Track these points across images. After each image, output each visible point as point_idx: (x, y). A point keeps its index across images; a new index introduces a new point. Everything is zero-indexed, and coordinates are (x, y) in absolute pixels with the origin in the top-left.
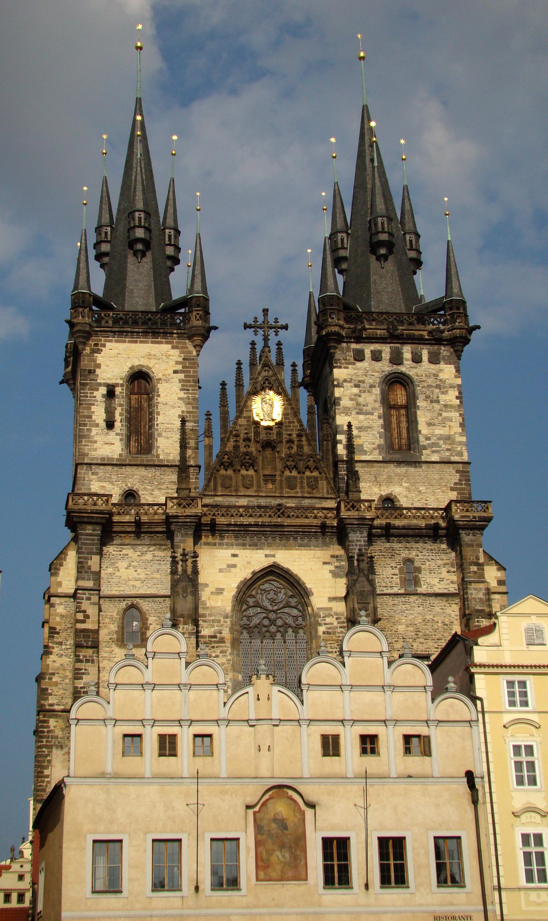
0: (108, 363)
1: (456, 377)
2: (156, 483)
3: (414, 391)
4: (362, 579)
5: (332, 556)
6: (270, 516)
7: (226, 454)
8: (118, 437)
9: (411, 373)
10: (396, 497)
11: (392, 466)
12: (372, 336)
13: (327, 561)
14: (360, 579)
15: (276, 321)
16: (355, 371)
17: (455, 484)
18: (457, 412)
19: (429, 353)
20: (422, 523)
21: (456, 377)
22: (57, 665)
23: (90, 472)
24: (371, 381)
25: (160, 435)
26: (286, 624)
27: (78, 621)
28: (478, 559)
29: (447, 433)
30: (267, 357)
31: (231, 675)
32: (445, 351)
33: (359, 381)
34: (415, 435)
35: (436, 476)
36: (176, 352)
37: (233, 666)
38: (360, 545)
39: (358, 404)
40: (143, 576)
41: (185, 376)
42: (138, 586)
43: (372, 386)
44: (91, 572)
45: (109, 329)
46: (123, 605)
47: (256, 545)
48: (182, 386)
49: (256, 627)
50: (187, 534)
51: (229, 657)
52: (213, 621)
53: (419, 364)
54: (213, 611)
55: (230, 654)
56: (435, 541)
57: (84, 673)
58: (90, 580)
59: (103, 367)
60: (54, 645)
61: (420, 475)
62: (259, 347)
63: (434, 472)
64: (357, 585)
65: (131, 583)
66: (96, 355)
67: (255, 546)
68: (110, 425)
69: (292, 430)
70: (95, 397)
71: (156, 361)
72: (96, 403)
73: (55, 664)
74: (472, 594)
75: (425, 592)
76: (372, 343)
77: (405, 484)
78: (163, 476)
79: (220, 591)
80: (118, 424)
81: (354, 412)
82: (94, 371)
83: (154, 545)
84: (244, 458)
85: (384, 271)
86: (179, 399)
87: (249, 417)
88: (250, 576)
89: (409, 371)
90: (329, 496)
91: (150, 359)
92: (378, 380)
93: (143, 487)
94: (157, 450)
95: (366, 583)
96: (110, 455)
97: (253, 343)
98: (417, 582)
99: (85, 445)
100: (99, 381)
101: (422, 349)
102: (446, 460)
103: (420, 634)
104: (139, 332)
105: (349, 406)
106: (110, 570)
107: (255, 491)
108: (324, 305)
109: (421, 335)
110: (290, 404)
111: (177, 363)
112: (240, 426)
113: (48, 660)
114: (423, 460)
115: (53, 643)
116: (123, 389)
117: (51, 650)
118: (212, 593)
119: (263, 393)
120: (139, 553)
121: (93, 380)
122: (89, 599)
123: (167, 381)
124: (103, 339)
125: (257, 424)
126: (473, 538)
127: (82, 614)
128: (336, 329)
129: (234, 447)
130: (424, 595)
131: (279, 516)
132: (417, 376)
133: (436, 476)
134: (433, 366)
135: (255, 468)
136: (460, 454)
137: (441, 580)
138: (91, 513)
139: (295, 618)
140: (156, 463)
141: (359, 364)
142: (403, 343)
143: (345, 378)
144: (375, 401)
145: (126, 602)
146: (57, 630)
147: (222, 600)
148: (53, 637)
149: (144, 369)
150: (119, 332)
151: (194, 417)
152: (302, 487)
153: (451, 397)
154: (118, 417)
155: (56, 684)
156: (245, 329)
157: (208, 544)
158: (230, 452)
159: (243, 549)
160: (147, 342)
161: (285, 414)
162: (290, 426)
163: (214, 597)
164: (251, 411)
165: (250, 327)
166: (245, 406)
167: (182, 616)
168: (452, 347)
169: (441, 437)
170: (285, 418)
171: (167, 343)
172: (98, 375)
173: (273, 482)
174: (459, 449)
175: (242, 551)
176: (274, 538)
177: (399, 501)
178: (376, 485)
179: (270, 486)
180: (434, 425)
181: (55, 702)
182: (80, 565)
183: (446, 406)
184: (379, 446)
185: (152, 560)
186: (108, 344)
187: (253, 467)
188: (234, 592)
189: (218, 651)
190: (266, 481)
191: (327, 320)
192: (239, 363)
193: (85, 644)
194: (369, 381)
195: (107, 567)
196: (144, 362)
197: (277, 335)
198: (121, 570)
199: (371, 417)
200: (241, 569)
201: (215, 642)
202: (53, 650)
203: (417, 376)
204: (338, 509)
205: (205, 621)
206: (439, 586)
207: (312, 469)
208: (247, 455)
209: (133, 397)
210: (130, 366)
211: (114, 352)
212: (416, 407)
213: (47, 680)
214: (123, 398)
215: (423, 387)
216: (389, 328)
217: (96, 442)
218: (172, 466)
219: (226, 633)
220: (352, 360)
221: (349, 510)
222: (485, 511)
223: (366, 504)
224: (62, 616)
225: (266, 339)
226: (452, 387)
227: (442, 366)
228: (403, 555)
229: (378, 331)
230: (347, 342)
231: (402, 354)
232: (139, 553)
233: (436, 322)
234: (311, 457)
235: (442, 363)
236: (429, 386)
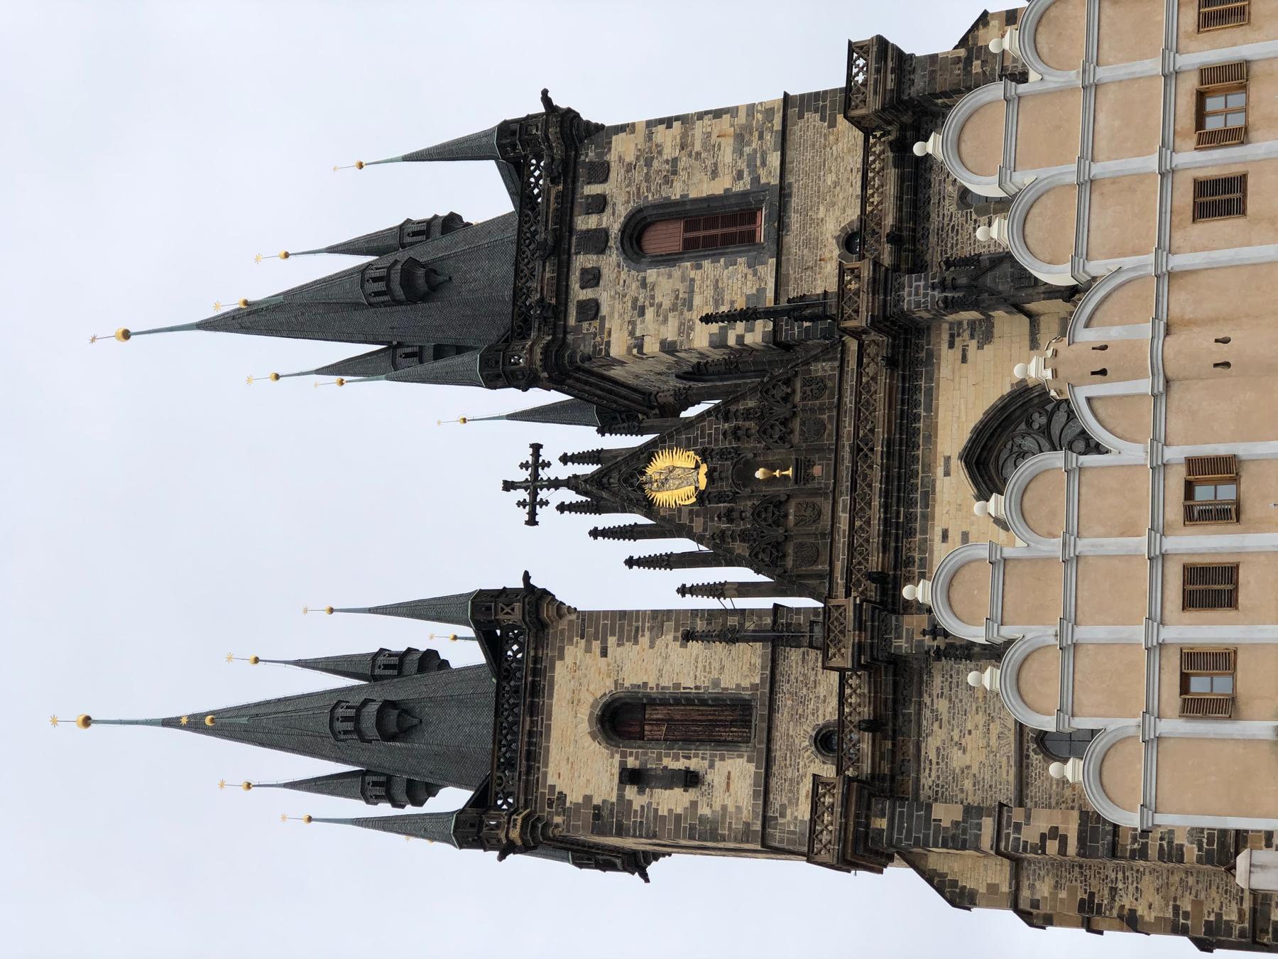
0: (583, 781)
1: (633, 132)
2: (805, 691)
4: (988, 280)
5: (951, 345)
6: (871, 467)
7: (756, 555)
8: (717, 764)
10: (844, 228)
12: (554, 288)
15: (524, 466)
16: (616, 315)
17: (823, 119)
18: (694, 123)
20: (892, 173)
22: (1157, 900)
23: (781, 821)
25: (716, 683)
27: (1063, 850)
29: (731, 141)
30: (586, 481)
32: (590, 155)
33: (634, 308)
34: (733, 201)
36: (570, 651)
38: (926, 288)
39: (674, 308)
40: (981, 719)
41: (613, 634)
42: (999, 729)
43: (644, 284)
44: (964, 821)
45: (524, 777)
46: (1036, 758)
47: (926, 495)
53: (609, 199)
57: (1170, 843)
58: (980, 824)
59: (588, 793)
60: (1117, 905)
61: (806, 186)
62: (570, 496)
63: (801, 159)
64: (1000, 288)
65: (994, 742)
66: (568, 804)
67: (928, 496)
68: (691, 779)
70: (642, 807)
71: (584, 689)
72: (654, 806)
73: (1156, 905)
76: (567, 286)
77: (821, 215)
78: (792, 677)
80: (694, 764)
81: (687, 315)
82: (596, 807)
83: (921, 695)
84: (765, 520)
85: (455, 276)
86: (652, 647)
87: (691, 512)
91: (579, 701)
92: (633, 272)
93: (811, 717)
94: (744, 689)
95: (997, 272)
96: (750, 781)
97: (562, 508)
99: (730, 827)
100: (614, 799)
104: (532, 722)
105: (676, 324)
106: (968, 784)
108: (499, 376)
110: (671, 436)
111: (588, 650)
112: (705, 530)
113: (1147, 919)
115: (1112, 908)
116: (631, 754)
117: (1126, 912)
119: (646, 487)
120: (936, 725)
121: (612, 811)
122: (1018, 828)
123: (620, 669)
124: (541, 790)
125: (702, 496)
126: (919, 72)
127: (1048, 842)
128: (538, 351)
129: (743, 540)
131: (872, 450)
132: (628, 202)
134: (613, 175)
135: (783, 498)
136: (769, 112)
138: (846, 817)
140: (767, 690)
141: (604, 311)
142: (571, 230)
143: (626, 333)
145: (1032, 754)
146: (1086, 897)
148: (1100, 906)
149: (597, 711)
150: (528, 760)
152: (822, 409)
154: (680, 764)
155: (1197, 903)
156: (536, 523)
158: (752, 548)
159: (933, 519)
164: (680, 509)
165: (533, 514)
166: (669, 520)
168: (581, 141)
169: (739, 151)
170: (695, 444)
171: (553, 668)
172: (604, 801)
173: (810, 464)
174: (760, 116)
175: (936, 522)
176: (915, 459)
177: (852, 222)
178: (821, 268)
179: (817, 470)
180: (716, 164)
181: (1234, 907)
182: (950, 844)
185: (950, 700)
186: (550, 782)
187: (781, 502)
190: (809, 478)
191: (522, 370)
192: (595, 533)
193: (1109, 838)
195: (962, 791)
196: (584, 712)
197: (549, 465)
198: (968, 763)
199: (697, 283)
200: (972, 524)
202: (1127, 907)
203: (628, 202)
204: (856, 334)
207: (789, 390)
208: (759, 515)
211: (564, 769)
212: (684, 201)
213: (1189, 922)
214: (645, 754)
215: (649, 190)
217: (724, 808)
218: (774, 661)
220: (596, 323)
221: (857, 312)
223: (847, 278)
224: (1057, 886)
225: (555, 484)
226: (649, 137)
227: (612, 157)
228: (953, 208)
229: (547, 275)
230: (565, 333)
231: (588, 231)
232: (936, 725)
233: (537, 173)
234: (766, 392)
235: (607, 158)
236: (647, 178)
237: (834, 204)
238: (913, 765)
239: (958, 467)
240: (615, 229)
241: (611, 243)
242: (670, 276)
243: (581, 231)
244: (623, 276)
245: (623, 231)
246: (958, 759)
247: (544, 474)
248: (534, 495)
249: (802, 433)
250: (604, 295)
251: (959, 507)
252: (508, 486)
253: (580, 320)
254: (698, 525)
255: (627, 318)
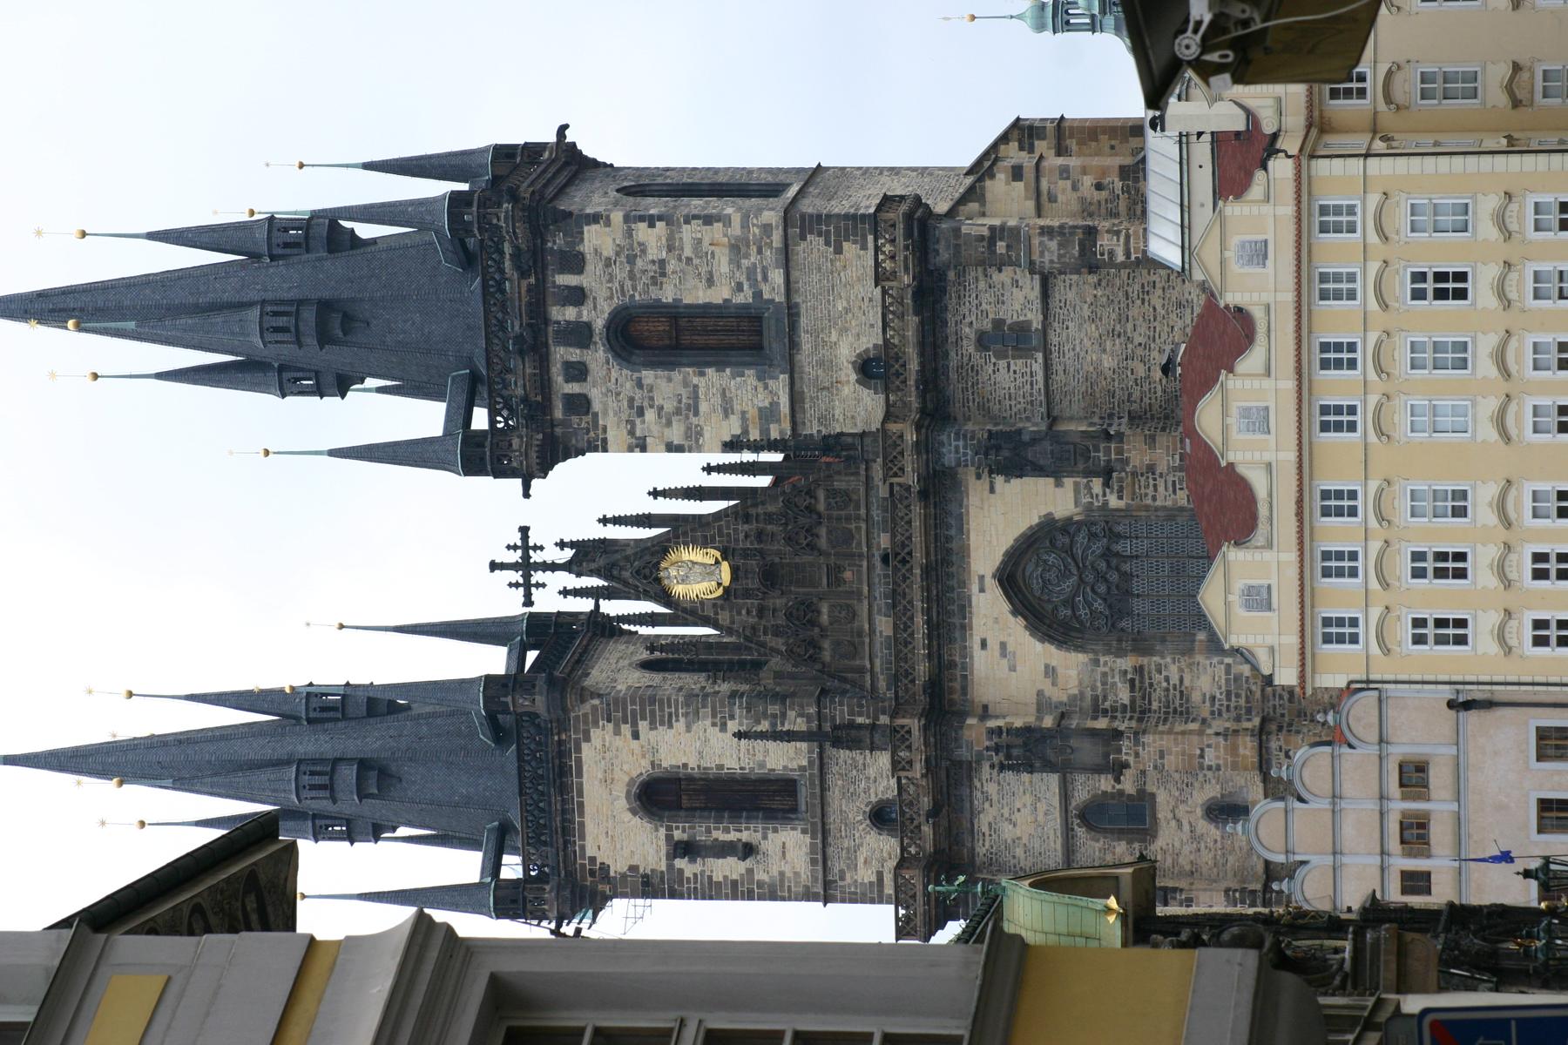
0: (626, 852)
1: (608, 223)
3: (641, 306)
8: (770, 835)
9: (607, 310)
10: (859, 355)
11: (798, 357)
13: (987, 487)
14: (1030, 456)
15: (515, 547)
16: (611, 413)
17: (827, 243)
19: (562, 272)
20: (913, 320)
21: (608, 223)
24: (628, 385)
25: (762, 765)
26: (1103, 555)
28: (982, 238)
31: (1199, 658)
32: (558, 242)
33: (631, 406)
35: (815, 277)
36: (595, 734)
37: (1183, 654)
38: (965, 447)
39: (678, 412)
40: (1028, 799)
41: (643, 718)
46: (1080, 832)
48: (662, 724)
49: (1110, 607)
50: (956, 739)
51: (1169, 660)
52: (1104, 683)
54: (1086, 681)
55: (1163, 657)
56: (944, 291)
63: (809, 284)
64: (1042, 462)
65: (1041, 818)
66: (612, 874)
67: (964, 608)
68: (748, 850)
69: (735, 530)
70: (695, 875)
74: (1052, 261)
75: (1041, 317)
77: (834, 337)
79: (1050, 672)
80: (745, 836)
81: (694, 420)
82: (645, 876)
83: (971, 780)
86: (688, 729)
87: (715, 605)
88: (1021, 621)
89: (602, 312)
90: (863, 472)
92: (625, 372)
95: (1037, 448)
96: (806, 849)
98: (1022, 329)
101: (554, 285)
102: (783, 257)
103: (1118, 327)
105: (682, 429)
106: (1019, 852)
107: (860, 600)
109: (529, 290)
111: (617, 732)
112: (733, 622)
114: (782, 299)
118: (1054, 684)
120: (987, 805)
123: (655, 751)
130: (1045, 317)
132: (611, 298)
133: (815, 277)
134: (589, 268)
136: (767, 229)
137: (1016, 283)
139: (1093, 536)
140: (816, 771)
141: (597, 406)
142: (547, 321)
144: (670, 380)
147: (1067, 668)
150: (564, 835)
151: (722, 705)
152: (848, 519)
153: (652, 238)
154: (732, 836)
157: (964, 690)
160: (580, 785)
161: (705, 545)
162: (729, 535)
163: (1060, 680)
164: (702, 602)
167: (1107, 755)
168: (546, 227)
169: (735, 262)
171: (578, 750)
174: (757, 231)
176: (950, 576)
177: (867, 350)
179: (848, 575)
180: (711, 273)
183: (670, 249)
184: (759, 379)
186: (589, 853)
188: (1052, 649)
189: (1157, 677)
194: (628, 387)
196: (620, 791)
197: (541, 548)
199: (701, 391)
201: (1142, 682)
205: (1105, 698)
206: (1027, 290)
209: (685, 802)
210: (630, 815)
211: (603, 841)
215: (634, 289)
216: (521, 353)
217: (782, 874)
219: (1127, 663)
221: (902, 469)
222: (893, 226)
225: (553, 567)
226: (629, 234)
227: (587, 247)
228: (971, 349)
229: (528, 371)
231: (568, 323)
232: (987, 805)
236: (632, 276)
237: (844, 331)
238: (967, 837)
239: (991, 583)
240: (599, 324)
241: (596, 338)
242: (670, 380)
243: (558, 323)
244: (614, 374)
245: (609, 326)
246: (1008, 832)
247: (536, 557)
248: (527, 577)
249: (829, 541)
250: (595, 394)
251: (996, 620)
252: (494, 566)
253: (564, 414)
254: (724, 618)
255: (624, 417)
